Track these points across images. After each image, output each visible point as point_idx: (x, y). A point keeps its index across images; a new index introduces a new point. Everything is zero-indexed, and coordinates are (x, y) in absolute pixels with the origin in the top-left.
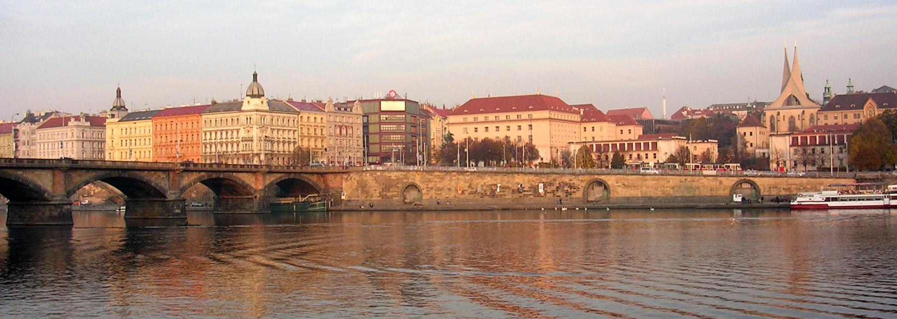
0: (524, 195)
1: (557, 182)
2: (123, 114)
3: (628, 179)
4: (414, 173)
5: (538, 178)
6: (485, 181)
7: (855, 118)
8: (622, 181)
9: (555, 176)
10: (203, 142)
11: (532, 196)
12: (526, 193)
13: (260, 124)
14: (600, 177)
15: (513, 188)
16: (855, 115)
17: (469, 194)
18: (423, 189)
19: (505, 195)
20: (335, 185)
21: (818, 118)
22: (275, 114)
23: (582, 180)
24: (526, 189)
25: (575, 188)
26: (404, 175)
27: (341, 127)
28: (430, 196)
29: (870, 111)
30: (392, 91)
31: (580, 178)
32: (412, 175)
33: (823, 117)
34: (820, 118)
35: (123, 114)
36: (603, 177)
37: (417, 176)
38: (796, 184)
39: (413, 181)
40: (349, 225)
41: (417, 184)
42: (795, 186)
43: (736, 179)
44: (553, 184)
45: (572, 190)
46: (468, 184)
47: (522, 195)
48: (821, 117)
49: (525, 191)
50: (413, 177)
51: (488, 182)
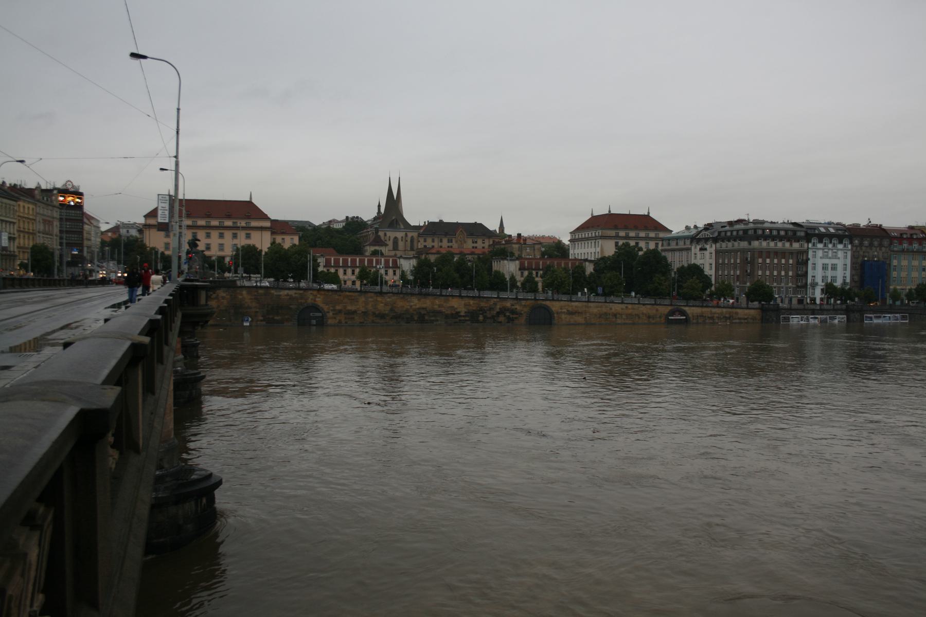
0: (460, 320)
1: (498, 307)
3: (572, 306)
4: (315, 293)
5: (475, 302)
6: (412, 304)
7: (449, 242)
8: (567, 307)
9: (495, 300)
11: (469, 322)
12: (463, 318)
14: (544, 303)
15: (446, 312)
16: (448, 240)
17: (391, 318)
18: (328, 312)
23: (525, 305)
24: (462, 314)
25: (517, 314)
26: (301, 294)
28: (337, 321)
30: (69, 181)
31: (523, 303)
32: (311, 294)
33: (423, 240)
34: (421, 240)
36: (548, 303)
38: (718, 313)
41: (319, 306)
42: (717, 315)
43: (670, 308)
44: (493, 309)
45: (514, 316)
46: (390, 307)
48: (422, 240)
49: (461, 316)
51: (416, 305)
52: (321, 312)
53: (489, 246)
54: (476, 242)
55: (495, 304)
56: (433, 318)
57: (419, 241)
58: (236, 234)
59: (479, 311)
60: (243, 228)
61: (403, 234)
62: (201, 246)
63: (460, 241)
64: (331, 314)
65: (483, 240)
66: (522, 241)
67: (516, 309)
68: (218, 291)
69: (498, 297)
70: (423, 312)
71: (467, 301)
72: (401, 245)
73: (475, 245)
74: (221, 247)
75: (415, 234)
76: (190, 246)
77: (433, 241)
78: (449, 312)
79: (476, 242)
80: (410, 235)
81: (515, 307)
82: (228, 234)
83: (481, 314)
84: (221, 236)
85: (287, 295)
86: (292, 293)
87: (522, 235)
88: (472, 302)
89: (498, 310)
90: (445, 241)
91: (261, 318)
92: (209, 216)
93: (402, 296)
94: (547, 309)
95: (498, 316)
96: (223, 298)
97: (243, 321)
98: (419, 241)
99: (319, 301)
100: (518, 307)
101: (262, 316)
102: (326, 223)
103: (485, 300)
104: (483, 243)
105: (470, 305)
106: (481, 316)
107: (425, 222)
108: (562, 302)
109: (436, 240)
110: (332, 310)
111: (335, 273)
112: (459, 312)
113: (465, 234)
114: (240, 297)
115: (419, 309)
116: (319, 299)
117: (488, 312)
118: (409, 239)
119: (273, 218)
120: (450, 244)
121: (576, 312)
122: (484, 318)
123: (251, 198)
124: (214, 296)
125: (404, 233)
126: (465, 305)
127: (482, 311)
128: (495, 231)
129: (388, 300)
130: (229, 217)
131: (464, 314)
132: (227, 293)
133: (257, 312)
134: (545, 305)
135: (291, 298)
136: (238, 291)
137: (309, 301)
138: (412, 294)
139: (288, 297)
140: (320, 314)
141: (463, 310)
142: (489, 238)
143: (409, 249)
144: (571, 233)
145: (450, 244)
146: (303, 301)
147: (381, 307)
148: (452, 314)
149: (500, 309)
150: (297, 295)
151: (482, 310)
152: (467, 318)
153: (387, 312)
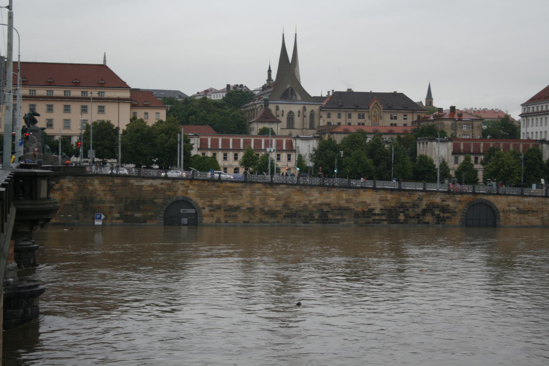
0: (374, 220)
4: (187, 183)
6: (312, 198)
7: (359, 118)
8: (516, 204)
9: (421, 194)
11: (385, 223)
14: (486, 198)
16: (359, 115)
17: (284, 216)
18: (204, 208)
21: (321, 115)
23: (459, 201)
24: (377, 212)
25: (450, 212)
26: (168, 184)
28: (215, 219)
29: (375, 112)
31: (458, 197)
32: (182, 184)
34: (323, 116)
36: (491, 198)
39: (184, 195)
40: (295, 286)
41: (191, 200)
44: (418, 205)
45: (446, 215)
46: (283, 202)
47: (370, 220)
49: (375, 215)
50: (185, 189)
51: (316, 200)
52: (193, 208)
53: (413, 122)
54: (396, 118)
55: (420, 199)
56: (339, 217)
57: (321, 117)
58: (86, 107)
59: (399, 207)
60: (96, 99)
61: (300, 108)
62: (41, 123)
63: (375, 116)
64: (206, 211)
65: (405, 115)
66: (456, 117)
67: (448, 205)
68: (62, 181)
69: (424, 190)
70: (325, 209)
71: (383, 194)
72: (298, 121)
73: (394, 121)
74: (67, 123)
75: (316, 108)
76: (26, 122)
77: (339, 116)
78: (359, 209)
79: (396, 118)
80: (309, 108)
81: (447, 203)
82: (76, 107)
83: (401, 212)
84: (67, 109)
85: (151, 186)
86: (157, 183)
87: (456, 108)
88: (389, 196)
89: (424, 207)
90: (355, 116)
91: (117, 215)
92: (50, 84)
93: (298, 187)
94: (490, 206)
95: (424, 215)
96: (69, 189)
97: (93, 219)
98: (321, 117)
99: (192, 193)
100: (451, 203)
101: (119, 213)
102: (202, 92)
103: (407, 193)
104: (405, 119)
105: (387, 200)
106: (402, 214)
107: (329, 92)
108: (510, 198)
109: (343, 115)
110: (209, 206)
111: (212, 157)
112: (373, 210)
113: (382, 108)
114: (91, 188)
115: (321, 204)
116: (192, 191)
117: (411, 209)
118: (308, 114)
119: (133, 87)
120: (361, 121)
121: (529, 211)
122: (406, 217)
123: (105, 61)
124: (57, 186)
125: (302, 106)
126: (381, 200)
127: (402, 207)
128: (421, 103)
129: (281, 192)
130: (76, 85)
131: (379, 212)
132: (74, 183)
133: (112, 207)
134: (486, 200)
135: (156, 189)
136: (88, 181)
137: (180, 194)
138: (312, 186)
139: (152, 189)
140: (193, 211)
141: (377, 207)
142: (413, 113)
143: (308, 127)
144: (523, 105)
145: (361, 121)
146: (171, 193)
147: (271, 202)
148: (364, 212)
149: (426, 205)
150: (163, 186)
151: (403, 207)
152: (383, 218)
153: (279, 209)
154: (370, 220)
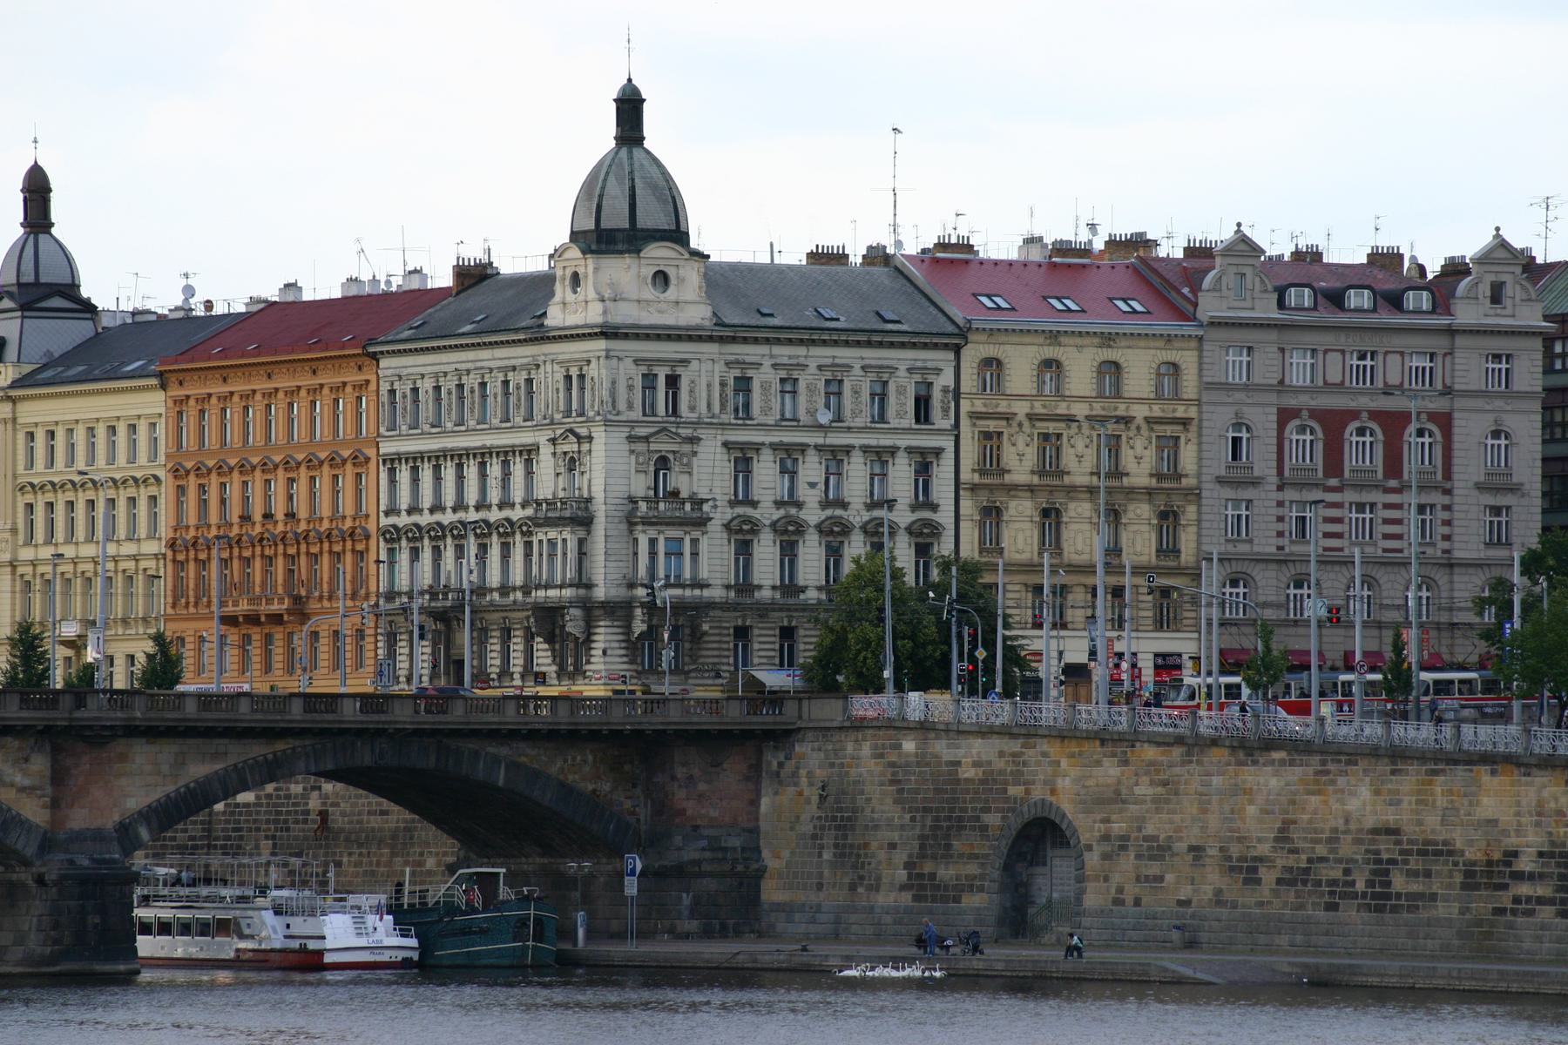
0: (1517, 900)
2: (67, 333)
6: (1353, 805)
10: (384, 521)
12: (1524, 889)
13: (637, 414)
19: (1433, 897)
20: (714, 813)
22: (763, 349)
24: (1525, 864)
27: (1333, 424)
35: (67, 333)
37: (1064, 763)
47: (1505, 899)
49: (1519, 876)
70: (1386, 848)
115: (1375, 831)
148: (1490, 863)
154: (1505, 899)
